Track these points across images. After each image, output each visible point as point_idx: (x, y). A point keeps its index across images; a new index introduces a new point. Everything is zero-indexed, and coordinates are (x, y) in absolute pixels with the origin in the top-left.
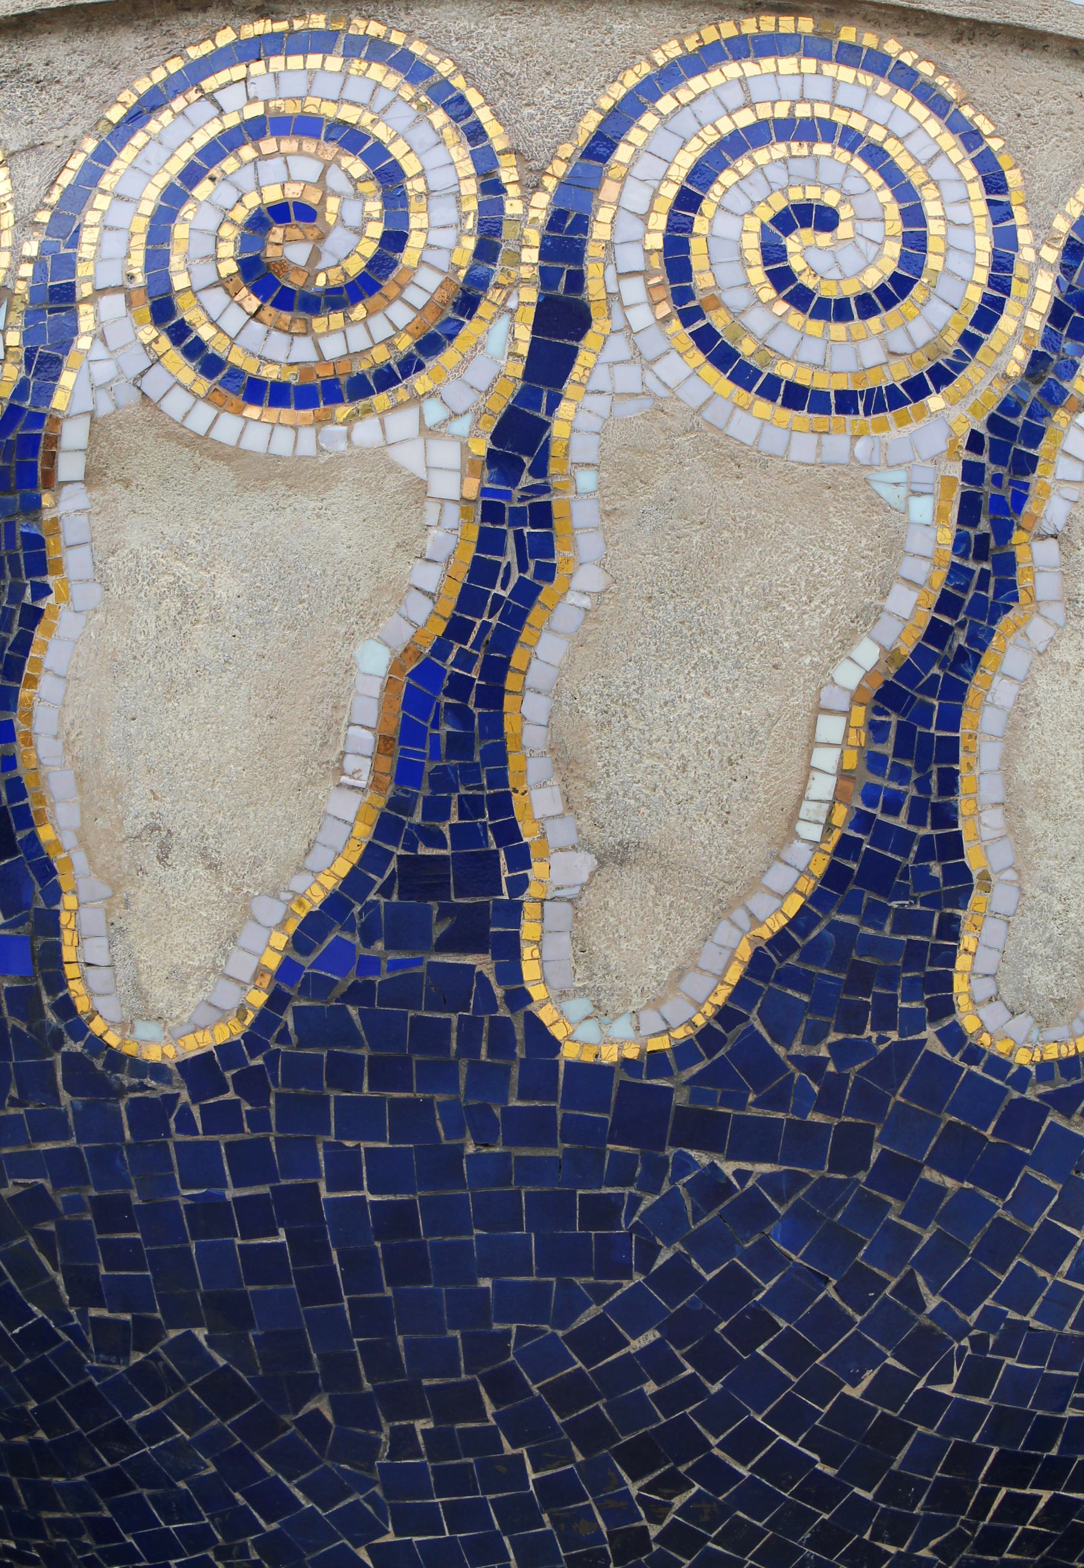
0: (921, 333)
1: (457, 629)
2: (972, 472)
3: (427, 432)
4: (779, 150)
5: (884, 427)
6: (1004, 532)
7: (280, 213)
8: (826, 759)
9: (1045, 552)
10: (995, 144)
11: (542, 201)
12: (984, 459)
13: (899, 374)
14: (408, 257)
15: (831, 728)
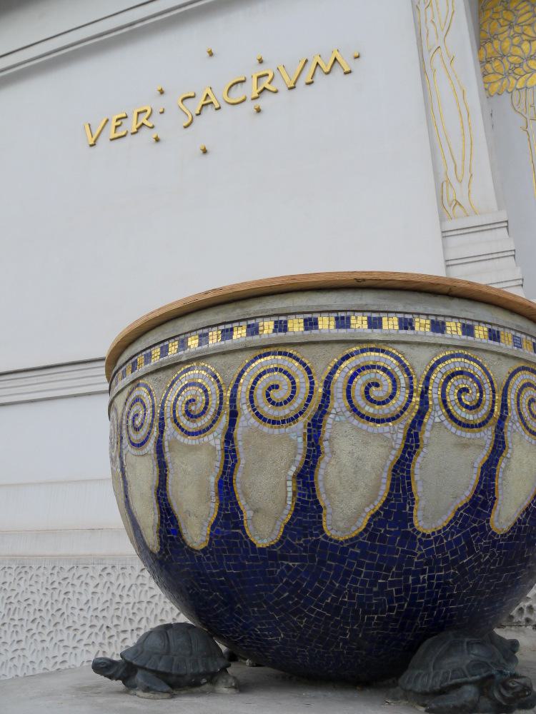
0: (296, 405)
1: (224, 473)
2: (309, 431)
3: (215, 438)
4: (268, 375)
5: (290, 425)
6: (317, 441)
7: (190, 401)
8: (290, 489)
9: (325, 444)
10: (309, 365)
11: (229, 392)
12: (311, 427)
13: (292, 415)
14: (209, 407)
15: (289, 483)
